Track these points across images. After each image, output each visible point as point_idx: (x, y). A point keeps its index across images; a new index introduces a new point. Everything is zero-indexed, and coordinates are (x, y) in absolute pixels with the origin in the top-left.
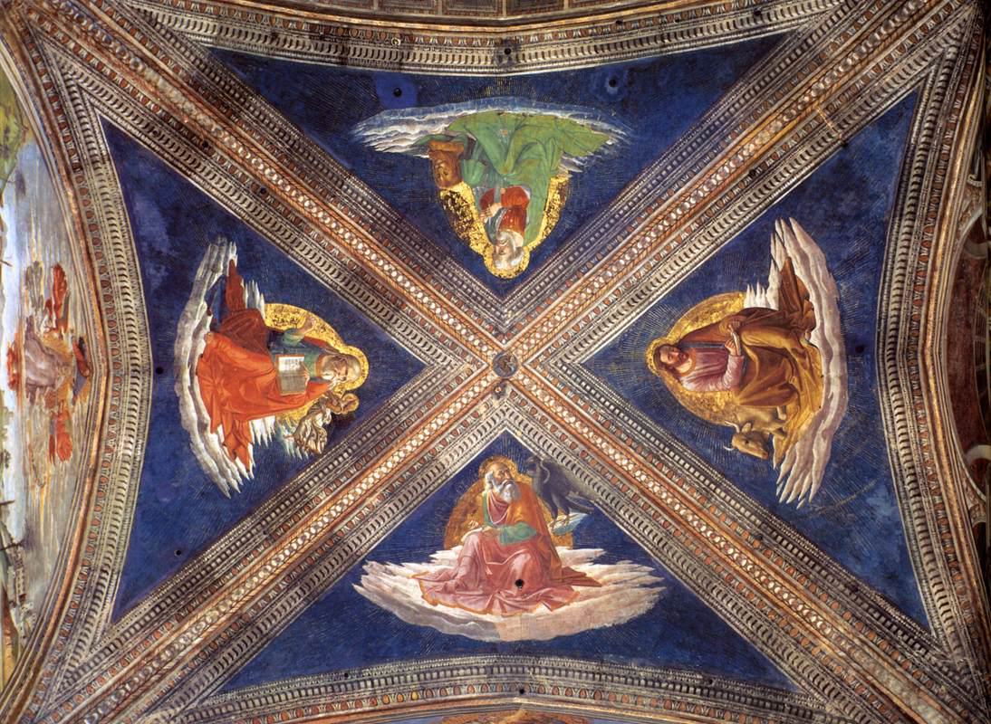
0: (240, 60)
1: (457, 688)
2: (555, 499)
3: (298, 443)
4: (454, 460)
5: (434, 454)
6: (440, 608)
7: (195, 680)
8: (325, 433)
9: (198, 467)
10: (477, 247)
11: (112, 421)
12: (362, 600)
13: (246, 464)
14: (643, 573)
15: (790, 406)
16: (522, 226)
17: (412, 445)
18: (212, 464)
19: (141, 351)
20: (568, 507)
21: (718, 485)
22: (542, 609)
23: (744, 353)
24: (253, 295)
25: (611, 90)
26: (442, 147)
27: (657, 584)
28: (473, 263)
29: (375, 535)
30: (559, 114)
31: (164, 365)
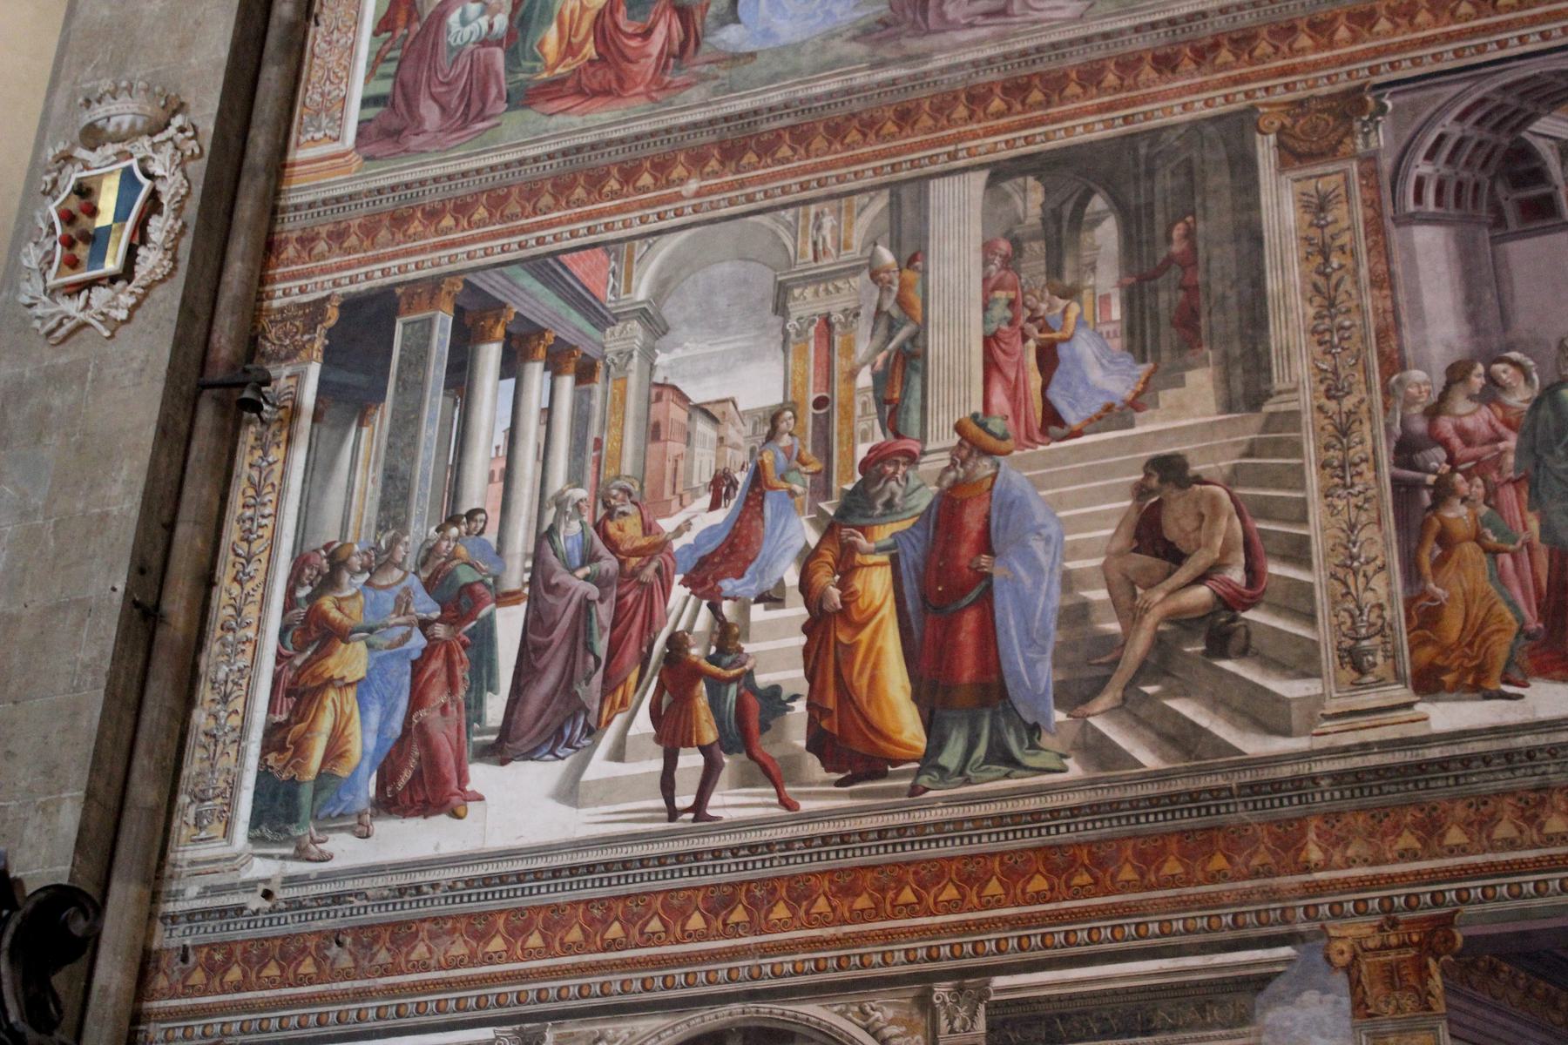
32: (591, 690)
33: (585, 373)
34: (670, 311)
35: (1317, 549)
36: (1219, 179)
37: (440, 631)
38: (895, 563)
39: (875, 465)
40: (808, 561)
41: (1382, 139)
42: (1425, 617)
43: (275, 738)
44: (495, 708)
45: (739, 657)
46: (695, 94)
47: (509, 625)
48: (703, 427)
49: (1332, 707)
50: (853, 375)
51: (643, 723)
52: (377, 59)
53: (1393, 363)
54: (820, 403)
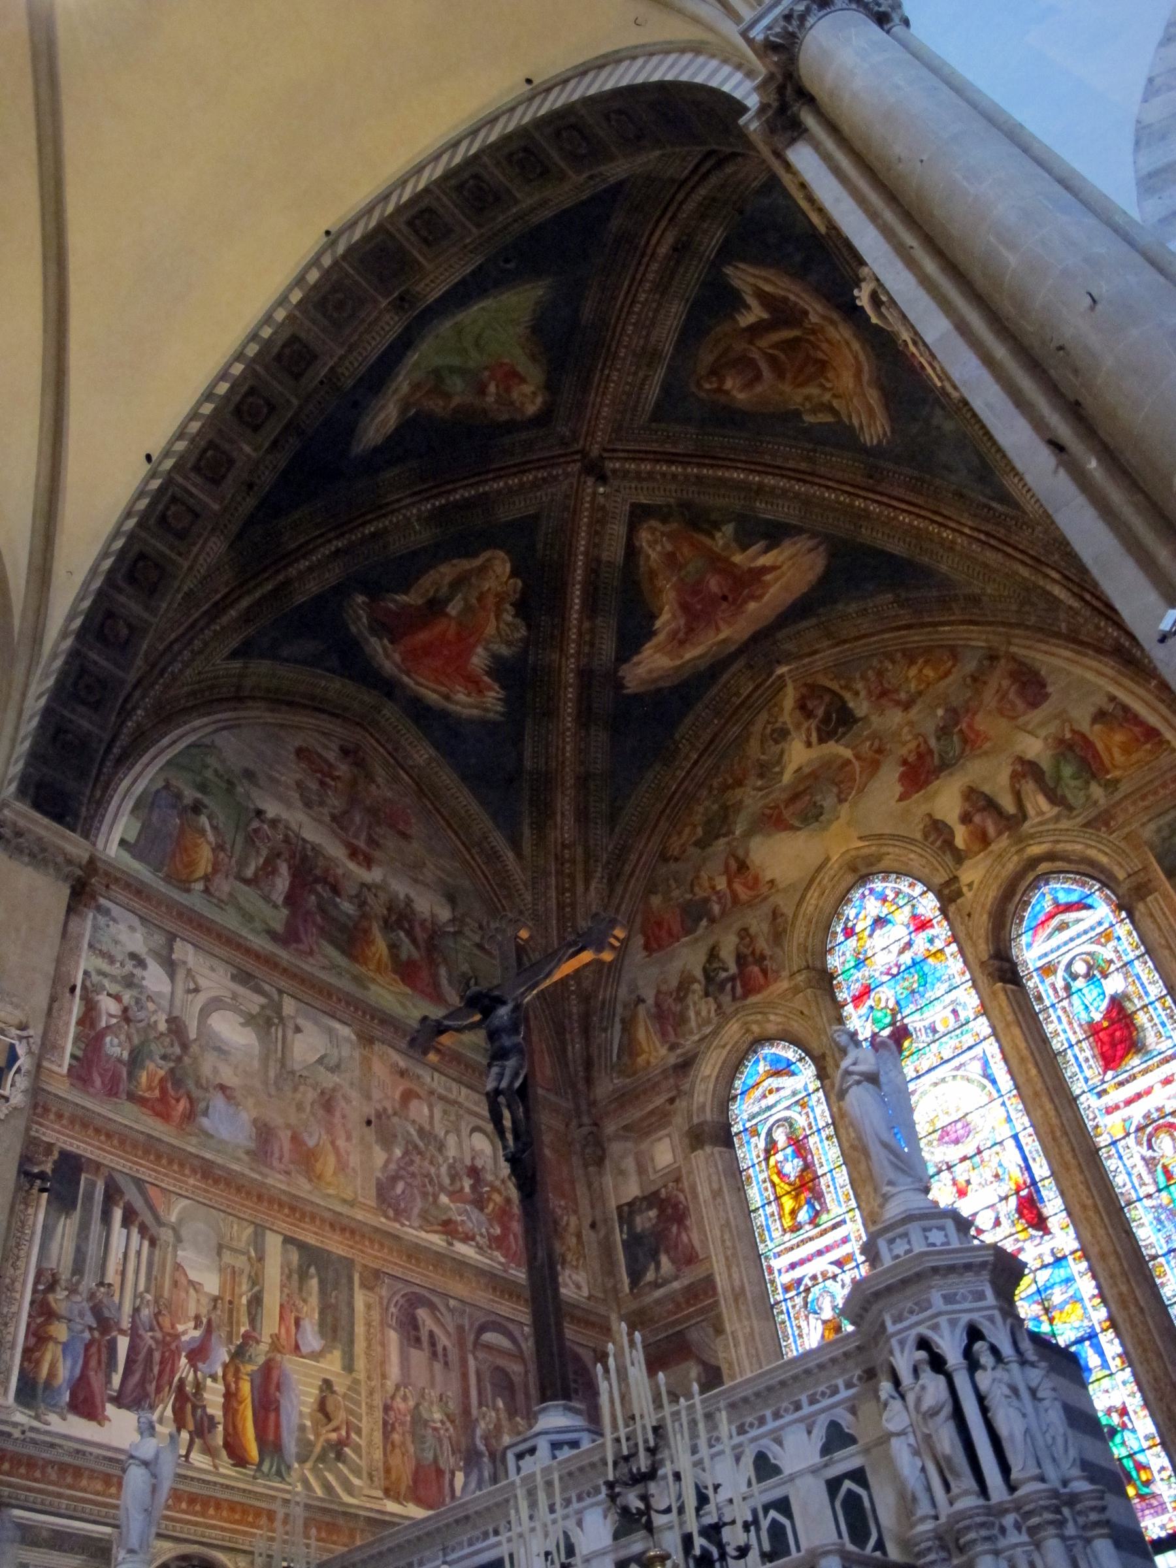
0: (250, 521)
1: (738, 694)
2: (705, 526)
3: (509, 644)
4: (614, 552)
5: (598, 560)
6: (688, 656)
7: (592, 842)
8: (518, 621)
9: (471, 721)
10: (505, 417)
11: (396, 750)
12: (636, 697)
13: (490, 689)
14: (804, 543)
15: (830, 375)
16: (523, 380)
17: (579, 575)
18: (475, 712)
19: (369, 697)
20: (716, 525)
21: (815, 451)
22: (752, 606)
23: (765, 354)
24: (395, 601)
25: (511, 266)
26: (418, 395)
27: (820, 544)
28: (511, 426)
29: (608, 647)
30: (481, 305)
31: (388, 687)
32: (151, 1388)
33: (153, 1243)
34: (184, 1232)
35: (364, 1432)
36: (344, 1281)
37: (96, 1334)
38: (252, 1382)
39: (246, 1336)
40: (226, 1366)
41: (384, 1292)
42: (388, 1471)
43: (27, 1352)
44: (116, 1379)
45: (202, 1399)
46: (194, 1140)
47: (123, 1344)
48: (192, 1291)
49: (367, 1492)
50: (240, 1296)
51: (169, 1413)
52: (77, 1039)
53: (384, 1376)
54: (231, 1302)
